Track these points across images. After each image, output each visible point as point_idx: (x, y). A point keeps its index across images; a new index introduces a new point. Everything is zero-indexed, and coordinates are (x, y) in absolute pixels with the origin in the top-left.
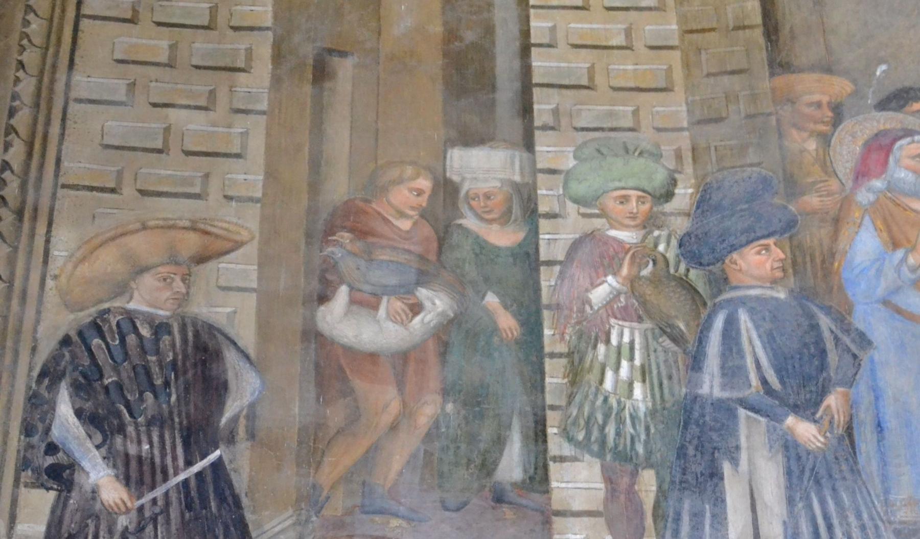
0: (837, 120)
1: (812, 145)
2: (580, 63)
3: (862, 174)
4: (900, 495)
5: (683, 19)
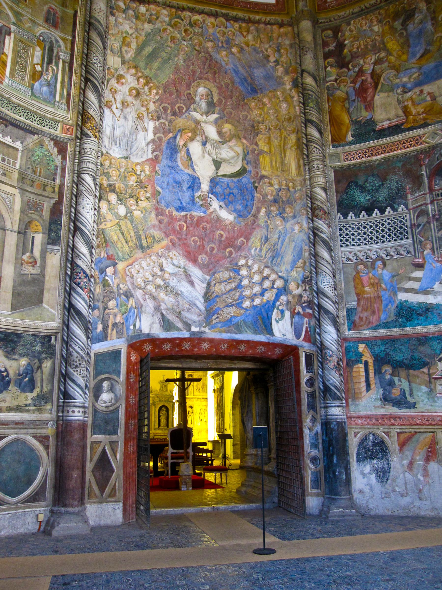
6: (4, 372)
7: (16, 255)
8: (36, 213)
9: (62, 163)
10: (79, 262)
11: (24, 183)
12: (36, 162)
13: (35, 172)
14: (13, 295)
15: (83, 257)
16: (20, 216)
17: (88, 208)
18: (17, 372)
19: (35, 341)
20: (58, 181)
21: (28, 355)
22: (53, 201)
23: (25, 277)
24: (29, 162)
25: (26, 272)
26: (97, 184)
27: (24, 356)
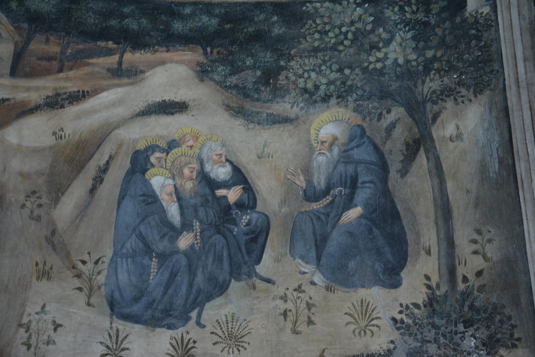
6: (227, 185)
18: (301, 181)
19: (379, 21)
21: (351, 90)
27: (326, 99)
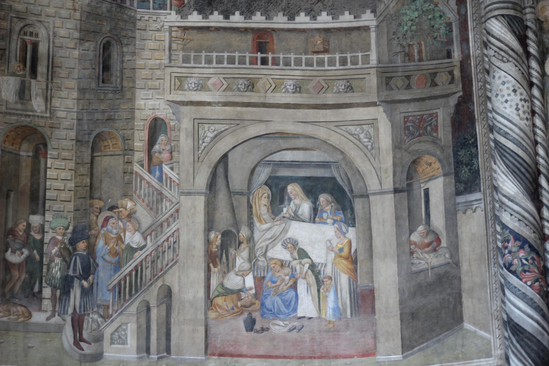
0: (100, 213)
1: (95, 218)
2: (55, 193)
3: (103, 226)
4: (99, 298)
5: (75, 183)
7: (397, 238)
8: (424, 138)
9: (459, 13)
10: (506, 218)
11: (392, 89)
12: (409, 34)
13: (409, 56)
14: (402, 320)
15: (510, 204)
16: (394, 157)
17: (505, 92)
20: (457, 55)
22: (453, 101)
23: (422, 277)
24: (395, 42)
25: (423, 266)
26: (527, 27)
